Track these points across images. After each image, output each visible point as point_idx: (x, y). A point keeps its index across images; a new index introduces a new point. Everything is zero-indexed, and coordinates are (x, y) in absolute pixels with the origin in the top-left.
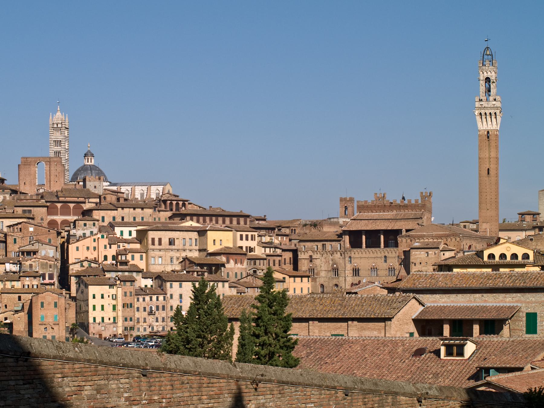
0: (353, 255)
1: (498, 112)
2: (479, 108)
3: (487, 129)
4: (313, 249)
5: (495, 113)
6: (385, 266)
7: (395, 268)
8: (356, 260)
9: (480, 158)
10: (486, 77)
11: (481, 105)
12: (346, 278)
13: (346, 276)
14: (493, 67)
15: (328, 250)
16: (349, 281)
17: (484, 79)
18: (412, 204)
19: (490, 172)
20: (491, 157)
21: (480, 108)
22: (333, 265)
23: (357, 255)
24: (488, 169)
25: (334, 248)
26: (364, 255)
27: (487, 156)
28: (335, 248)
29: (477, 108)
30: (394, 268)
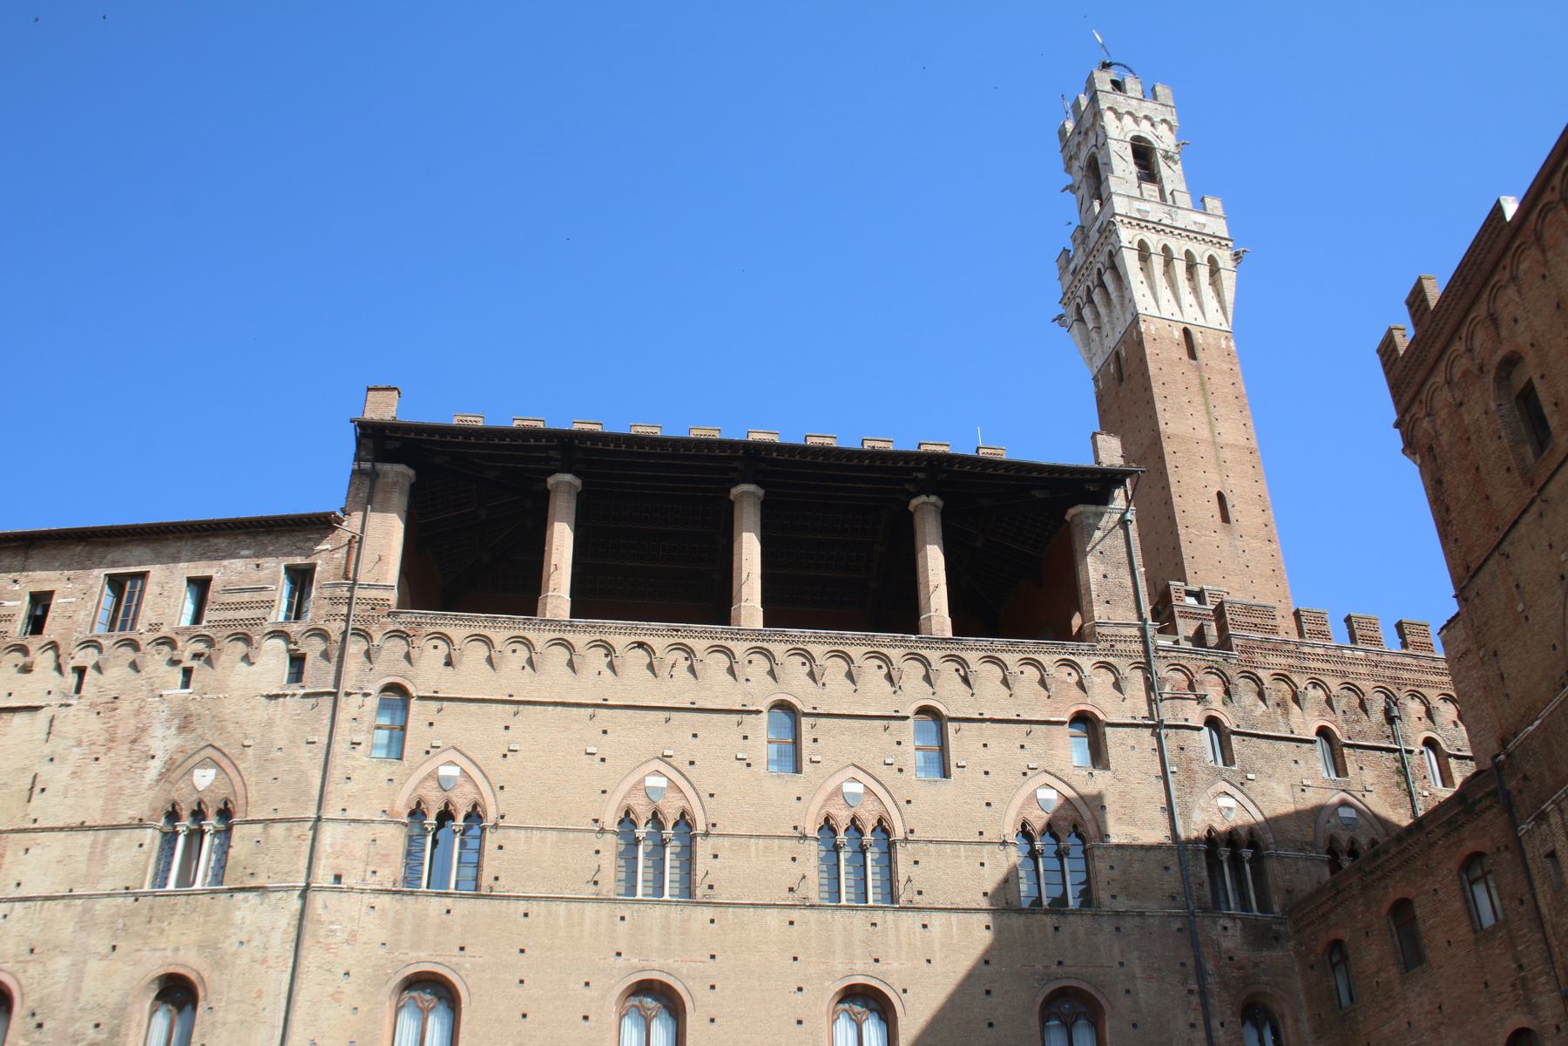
0: (427, 673)
1: (1225, 258)
2: (1134, 222)
3: (1178, 317)
5: (1212, 260)
7: (899, 833)
8: (456, 725)
10: (1136, 133)
11: (1139, 210)
12: (318, 901)
13: (323, 877)
14: (1159, 107)
15: (154, 627)
16: (352, 938)
17: (1128, 139)
19: (1233, 515)
20: (1218, 439)
21: (1141, 222)
22: (175, 769)
23: (473, 675)
24: (1220, 496)
25: (226, 606)
26: (554, 679)
27: (1203, 432)
28: (239, 606)
29: (1126, 220)
30: (882, 828)
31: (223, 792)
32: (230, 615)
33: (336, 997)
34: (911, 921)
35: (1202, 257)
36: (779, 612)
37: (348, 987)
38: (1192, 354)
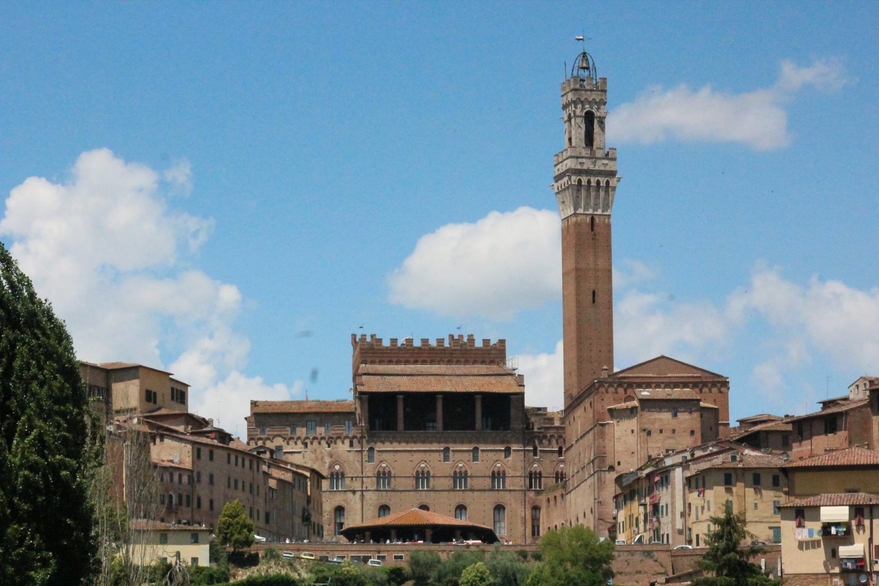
4: (286, 433)
6: (447, 468)
7: (469, 474)
8: (384, 455)
9: (577, 270)
11: (580, 163)
15: (321, 434)
16: (371, 499)
18: (478, 349)
23: (388, 447)
24: (594, 293)
27: (592, 266)
31: (341, 471)
32: (336, 432)
33: (369, 510)
34: (470, 493)
35: (603, 182)
36: (446, 427)
37: (371, 508)
38: (592, 230)
